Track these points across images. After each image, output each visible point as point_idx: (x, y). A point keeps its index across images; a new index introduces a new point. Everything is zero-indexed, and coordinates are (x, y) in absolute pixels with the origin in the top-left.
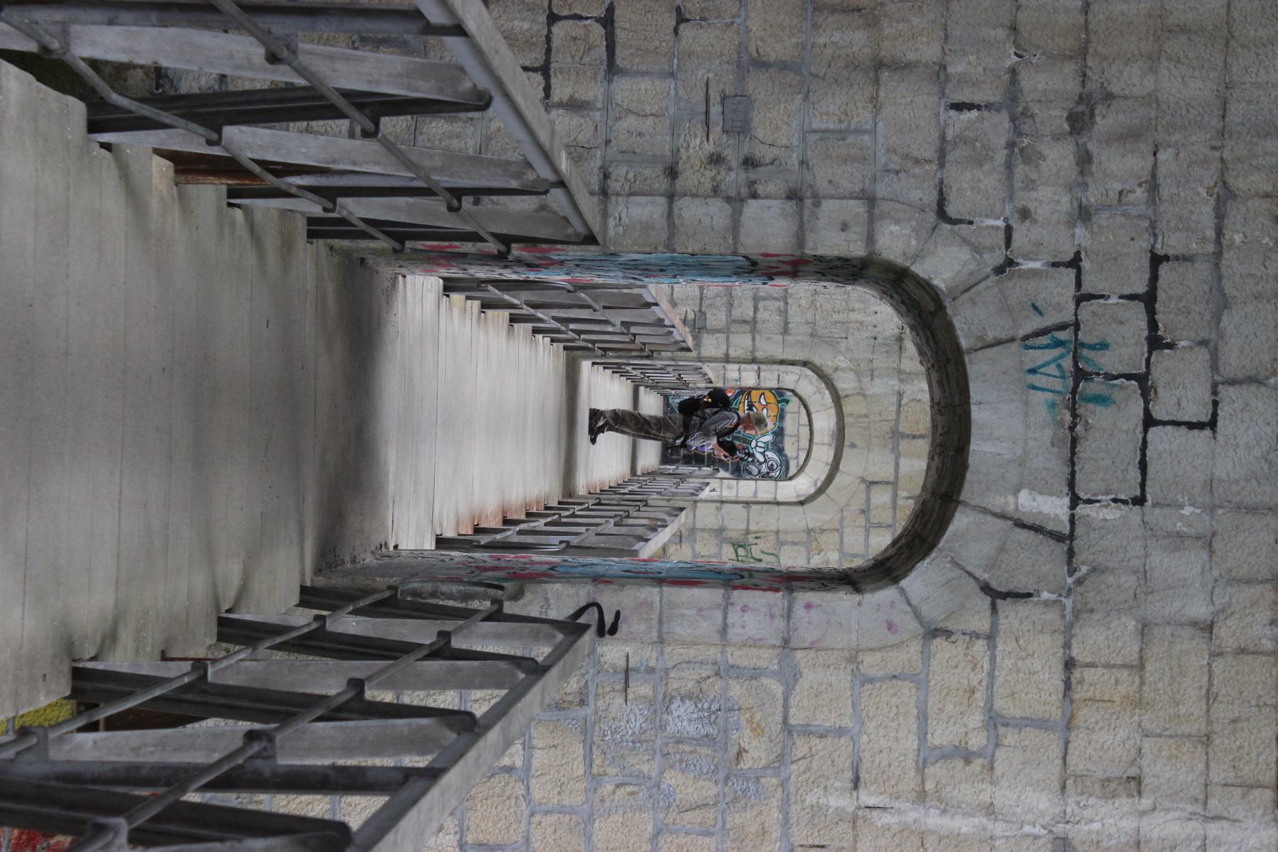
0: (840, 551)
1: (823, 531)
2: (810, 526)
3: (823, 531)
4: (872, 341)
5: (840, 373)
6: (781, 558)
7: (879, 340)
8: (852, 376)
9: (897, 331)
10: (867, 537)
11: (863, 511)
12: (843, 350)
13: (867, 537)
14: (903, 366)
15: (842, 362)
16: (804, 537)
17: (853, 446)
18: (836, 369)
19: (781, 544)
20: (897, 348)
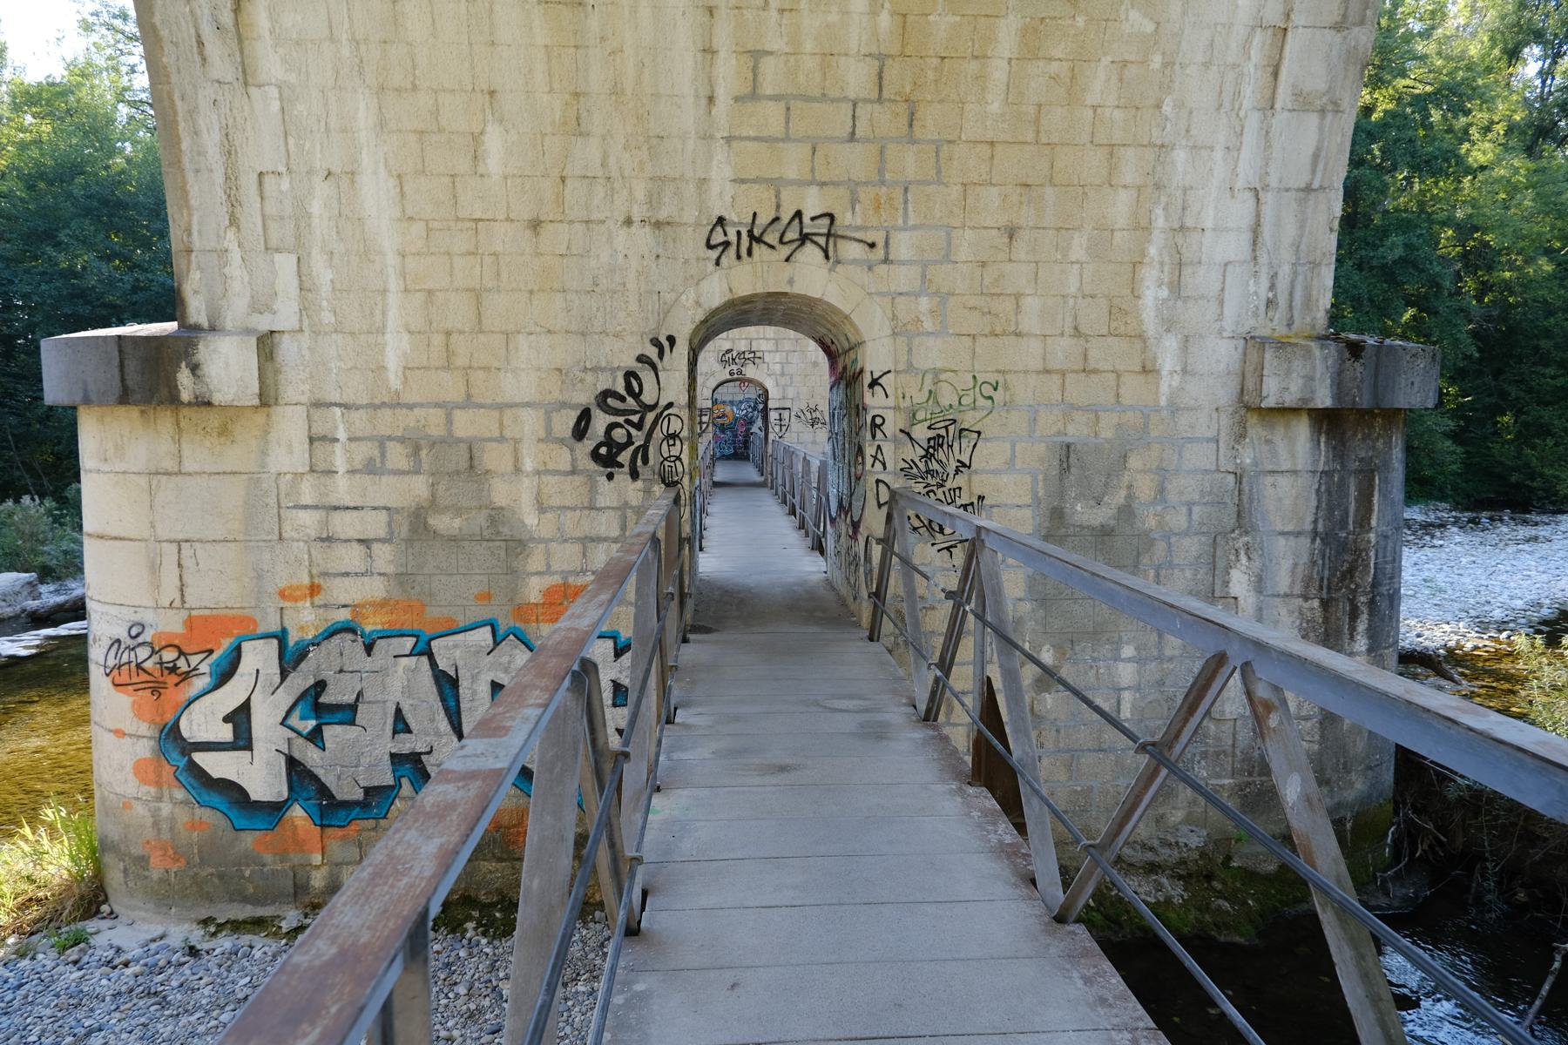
0: (917, 295)
1: (894, 317)
2: (889, 332)
3: (894, 317)
4: (661, 260)
5: (702, 300)
6: (927, 367)
7: (660, 251)
8: (705, 284)
9: (648, 229)
10: (903, 263)
11: (870, 268)
12: (674, 296)
13: (903, 263)
14: (692, 220)
15: (688, 298)
16: (901, 340)
17: (791, 282)
18: (698, 303)
19: (910, 367)
20: (668, 229)
